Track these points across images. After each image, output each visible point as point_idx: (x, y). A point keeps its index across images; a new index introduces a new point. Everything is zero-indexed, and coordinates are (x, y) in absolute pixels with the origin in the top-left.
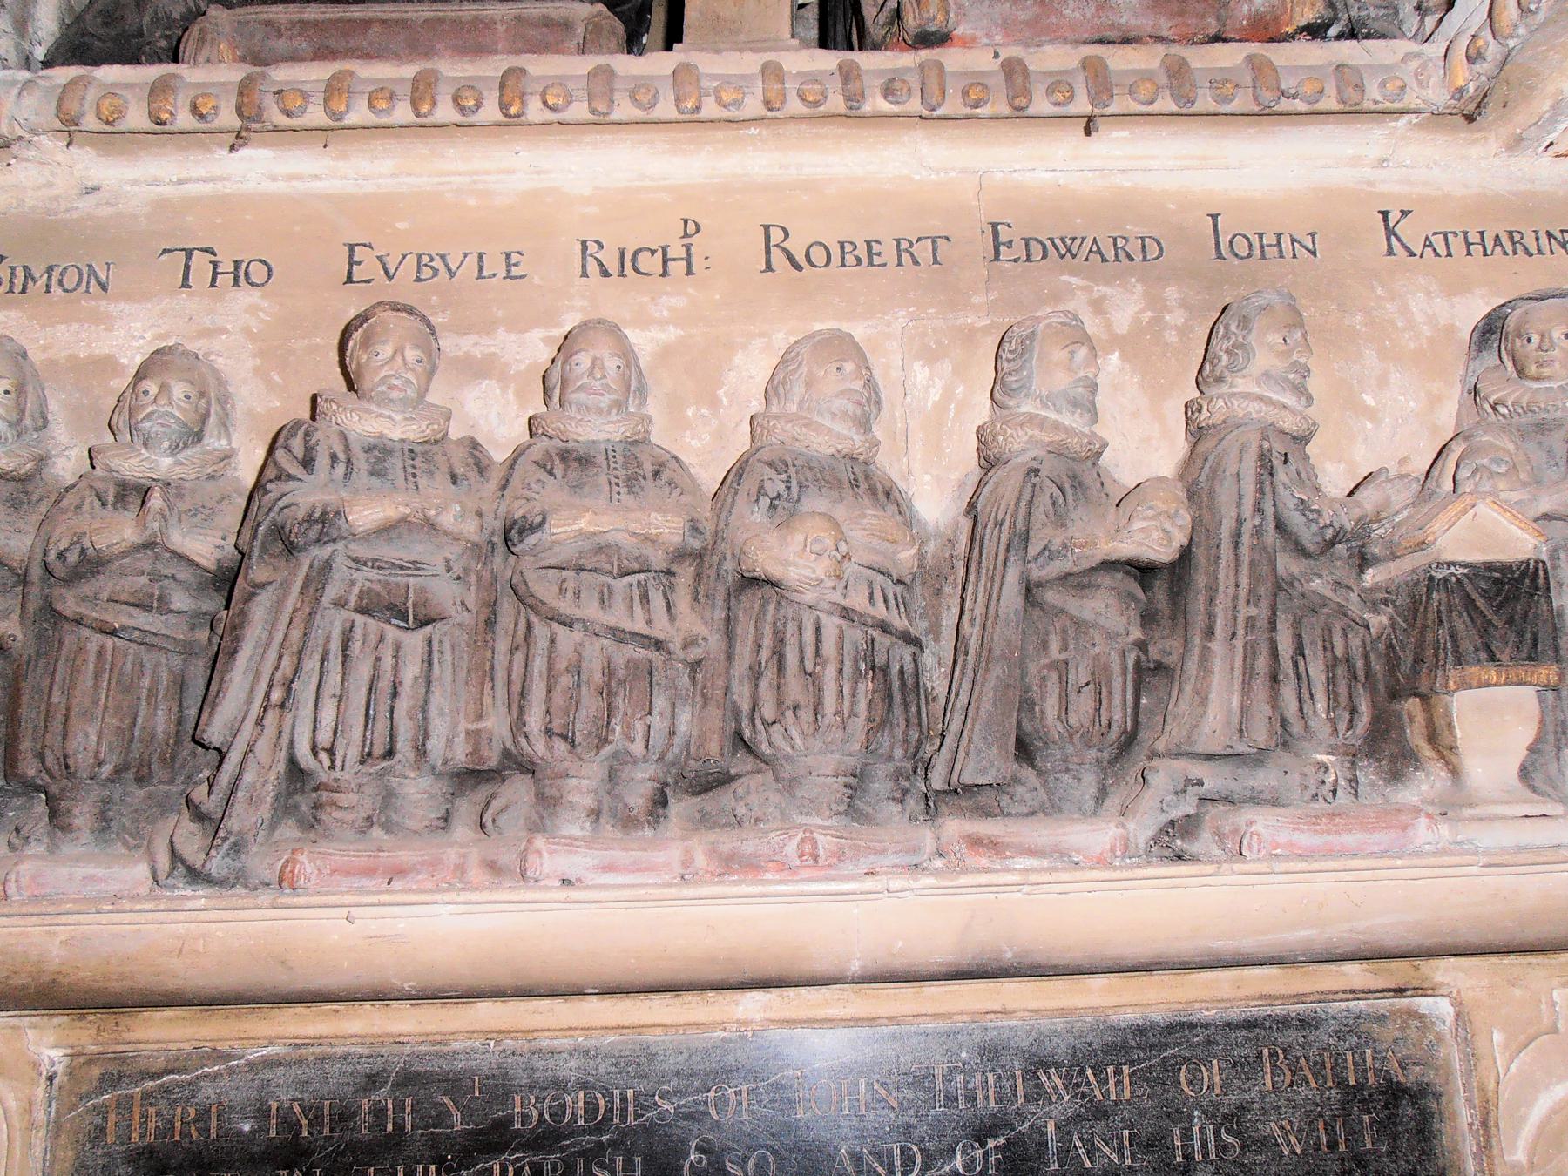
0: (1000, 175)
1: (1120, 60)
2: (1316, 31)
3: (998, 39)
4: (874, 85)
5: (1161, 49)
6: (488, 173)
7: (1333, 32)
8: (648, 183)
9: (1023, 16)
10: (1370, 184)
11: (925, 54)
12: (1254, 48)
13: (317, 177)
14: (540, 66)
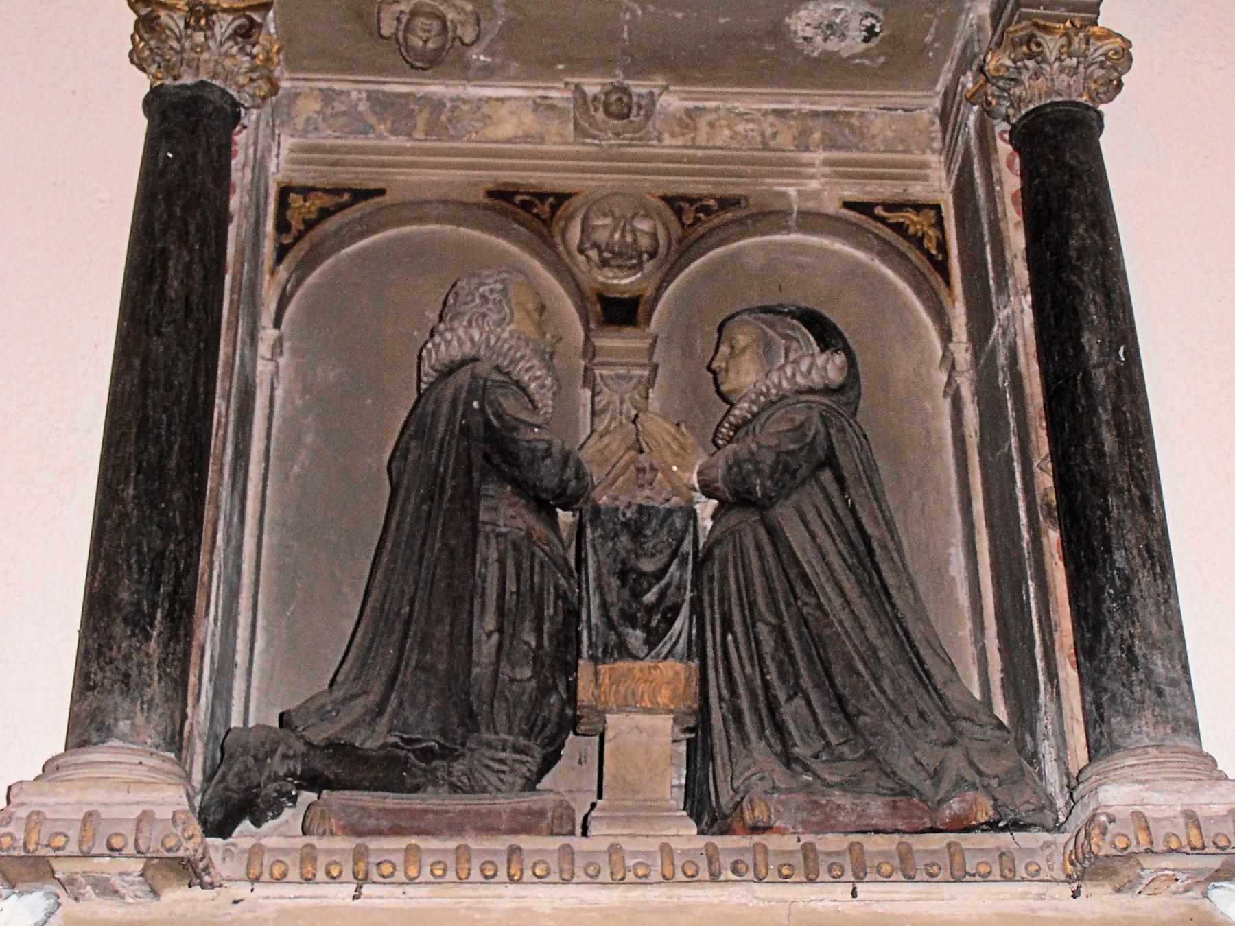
0: (802, 904)
1: (874, 843)
2: (992, 826)
3: (800, 830)
4: (726, 861)
5: (896, 837)
6: (487, 897)
7: (1001, 824)
8: (586, 906)
9: (814, 819)
10: (1033, 911)
11: (756, 838)
12: (952, 837)
13: (381, 897)
14: (527, 843)
